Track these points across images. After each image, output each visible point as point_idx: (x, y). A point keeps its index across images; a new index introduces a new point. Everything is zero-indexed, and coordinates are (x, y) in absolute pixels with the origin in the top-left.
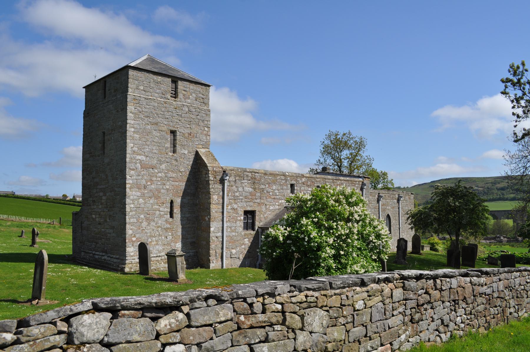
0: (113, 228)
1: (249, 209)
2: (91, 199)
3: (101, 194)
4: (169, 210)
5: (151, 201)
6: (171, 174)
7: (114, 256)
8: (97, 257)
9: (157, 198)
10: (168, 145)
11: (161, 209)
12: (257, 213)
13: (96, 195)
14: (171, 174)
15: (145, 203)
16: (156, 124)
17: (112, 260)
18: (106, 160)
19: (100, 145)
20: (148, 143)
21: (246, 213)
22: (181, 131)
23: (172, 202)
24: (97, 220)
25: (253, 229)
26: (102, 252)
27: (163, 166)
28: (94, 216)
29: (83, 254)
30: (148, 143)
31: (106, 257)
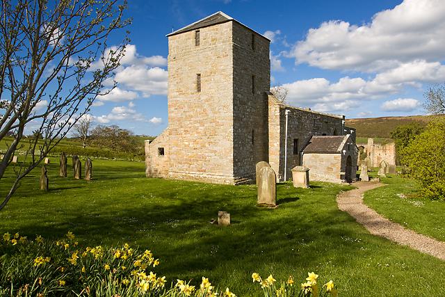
0: (216, 151)
1: (296, 138)
2: (182, 129)
3: (196, 125)
4: (251, 137)
5: (245, 131)
6: (253, 110)
7: (216, 174)
8: (192, 175)
9: (247, 128)
10: (251, 87)
11: (249, 137)
12: (299, 141)
13: (190, 126)
14: (253, 110)
15: (242, 132)
16: (246, 69)
17: (215, 177)
18: (203, 98)
19: (195, 85)
20: (243, 84)
21: (294, 140)
22: (258, 76)
23: (253, 131)
24: (191, 146)
25: (297, 154)
26: (199, 171)
27: (249, 104)
28: (187, 143)
29: (171, 173)
30: (243, 84)
31: (204, 175)
